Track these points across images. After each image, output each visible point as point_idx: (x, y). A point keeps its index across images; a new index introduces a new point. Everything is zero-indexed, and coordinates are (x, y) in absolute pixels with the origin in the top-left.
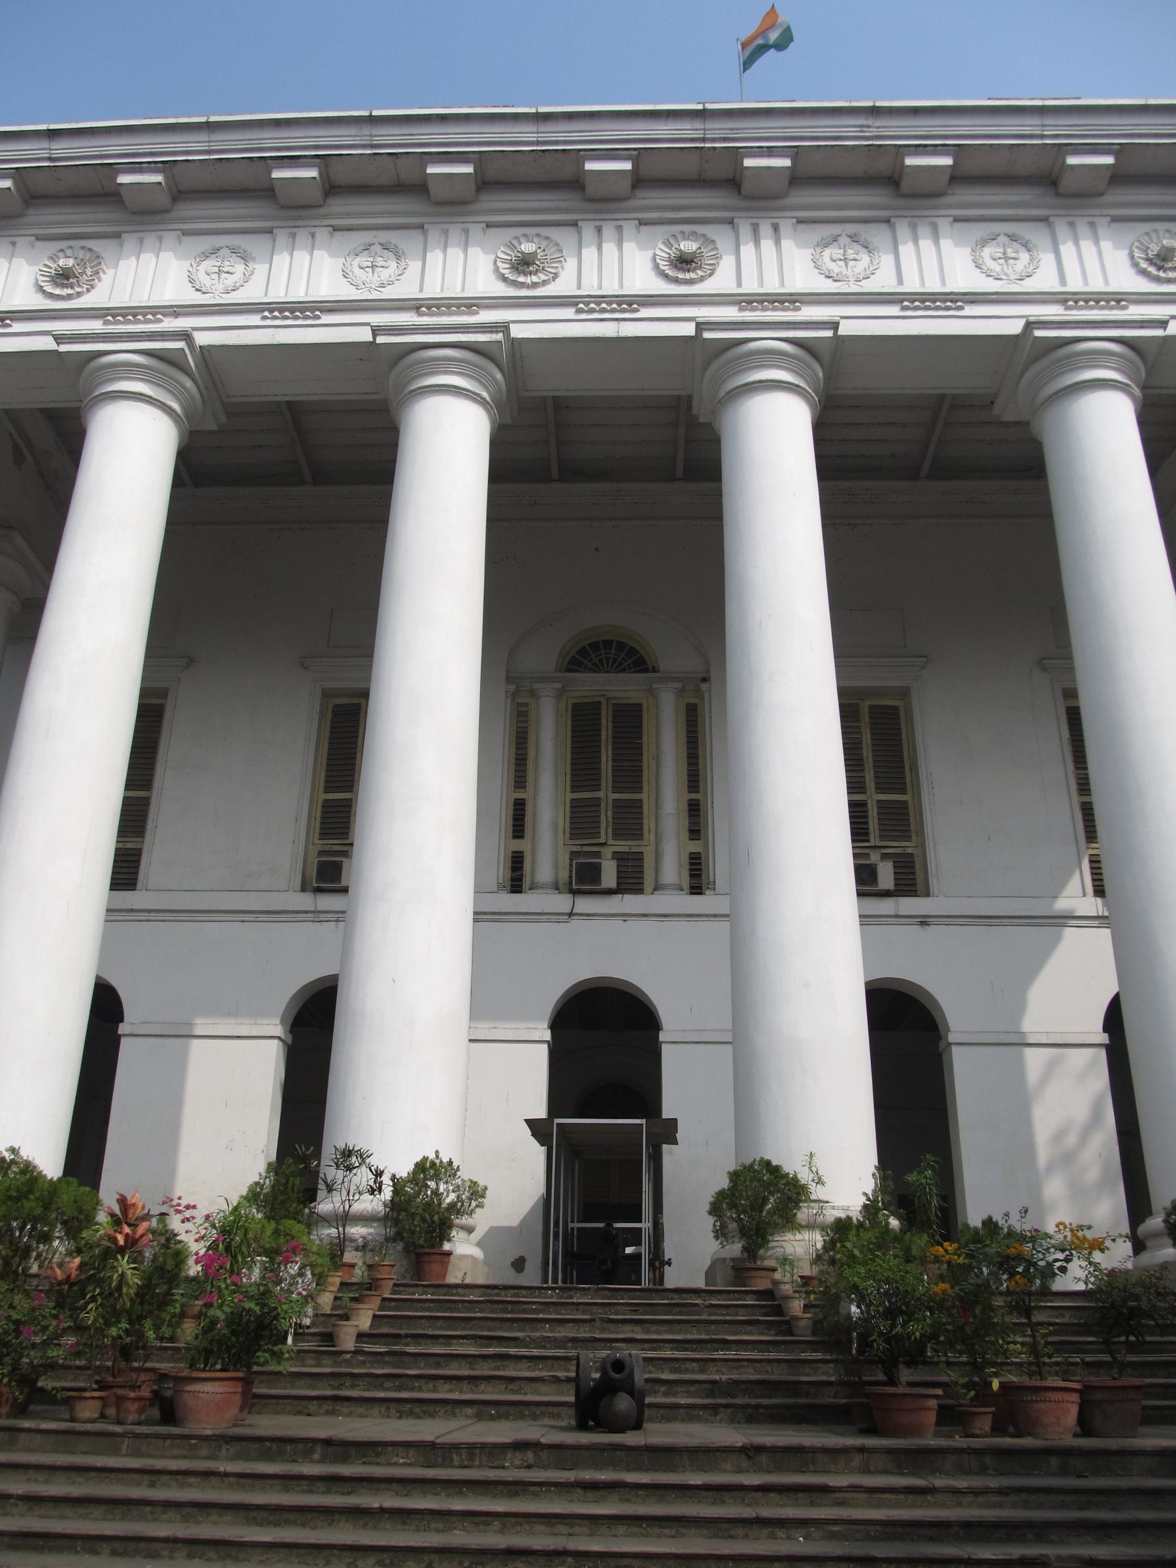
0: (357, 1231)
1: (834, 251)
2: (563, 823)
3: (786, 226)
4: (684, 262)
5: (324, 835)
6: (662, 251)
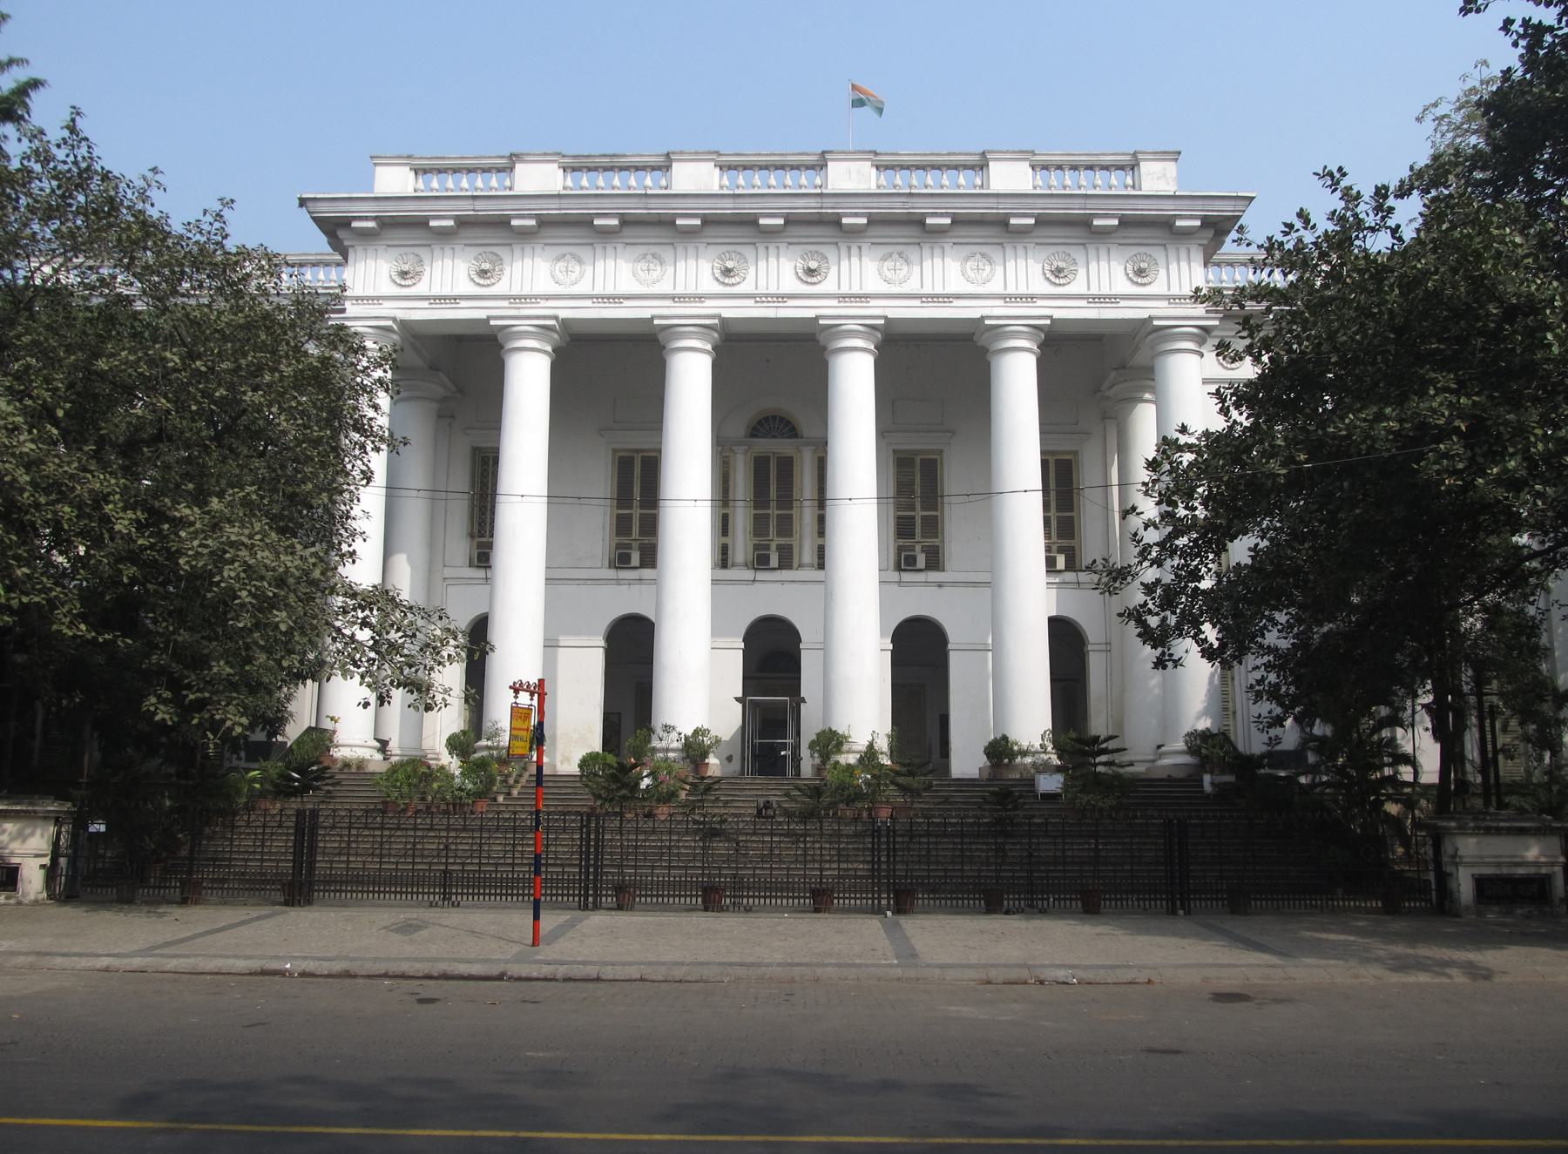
0: (671, 755)
1: (889, 264)
2: (750, 528)
3: (865, 247)
4: (810, 272)
5: (618, 534)
6: (800, 264)
